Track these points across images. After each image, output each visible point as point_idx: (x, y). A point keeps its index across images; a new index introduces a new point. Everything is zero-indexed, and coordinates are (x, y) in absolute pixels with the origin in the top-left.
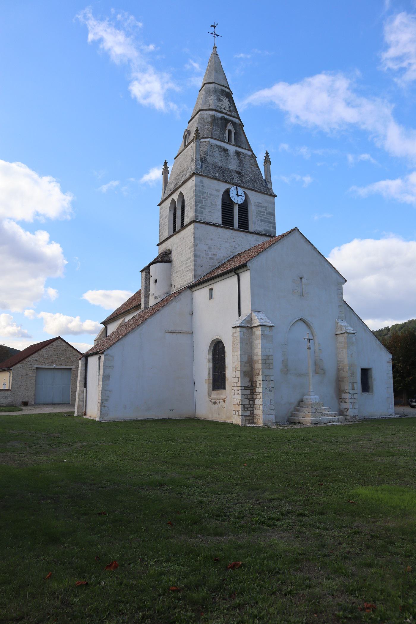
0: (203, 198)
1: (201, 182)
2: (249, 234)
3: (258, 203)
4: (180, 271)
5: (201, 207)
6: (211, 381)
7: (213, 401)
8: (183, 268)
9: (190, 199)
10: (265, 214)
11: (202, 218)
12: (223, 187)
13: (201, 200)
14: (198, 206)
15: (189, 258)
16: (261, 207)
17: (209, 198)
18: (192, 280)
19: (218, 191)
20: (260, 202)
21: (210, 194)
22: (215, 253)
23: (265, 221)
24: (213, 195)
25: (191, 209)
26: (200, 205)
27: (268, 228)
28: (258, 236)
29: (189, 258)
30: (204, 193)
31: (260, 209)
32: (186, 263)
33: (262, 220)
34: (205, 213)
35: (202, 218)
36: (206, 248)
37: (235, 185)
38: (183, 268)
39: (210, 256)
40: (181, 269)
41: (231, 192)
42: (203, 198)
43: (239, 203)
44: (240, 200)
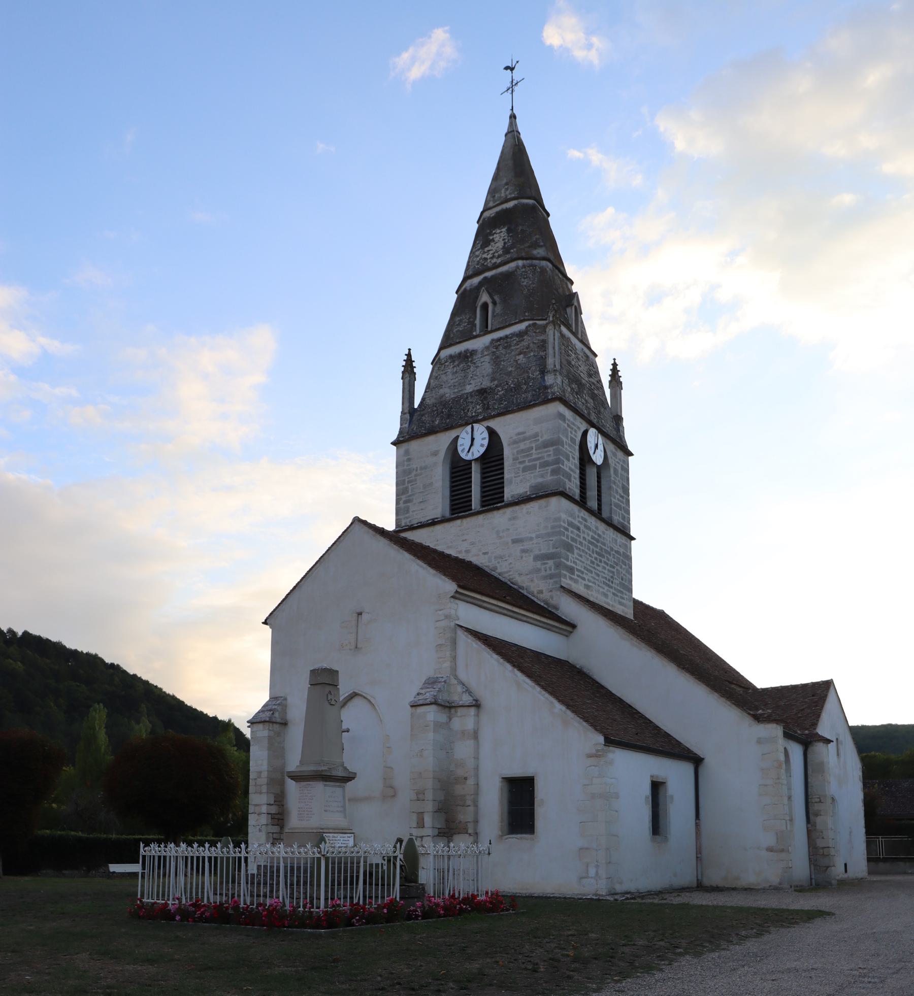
1: (407, 452)
2: (495, 513)
3: (519, 434)
5: (405, 502)
12: (443, 440)
13: (407, 488)
14: (401, 502)
16: (525, 439)
17: (418, 478)
19: (435, 454)
20: (521, 430)
21: (421, 468)
23: (534, 467)
24: (425, 468)
27: (540, 480)
28: (517, 508)
31: (522, 446)
33: (525, 469)
37: (467, 424)
41: (460, 441)
42: (409, 482)
43: (477, 455)
44: (479, 450)
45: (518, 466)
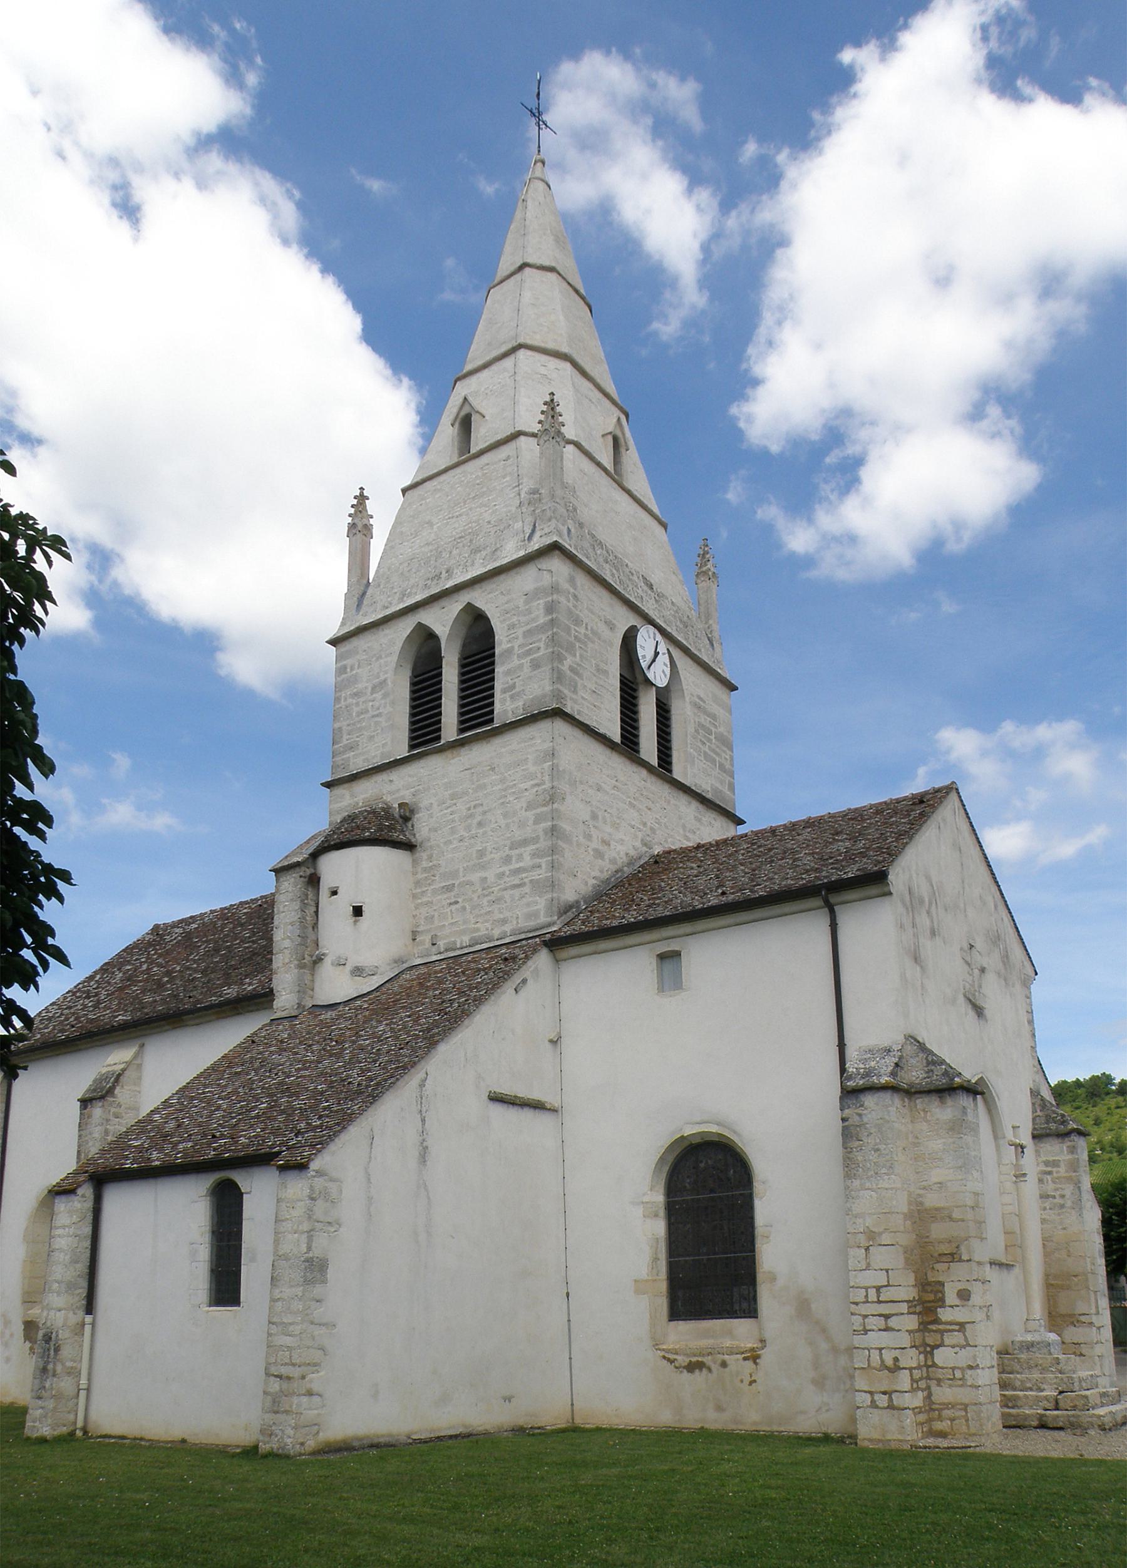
0: (576, 637)
4: (470, 883)
6: (663, 1286)
7: (682, 1360)
8: (491, 875)
9: (529, 633)
10: (713, 737)
11: (576, 707)
15: (525, 842)
17: (590, 645)
18: (543, 919)
22: (606, 837)
25: (536, 665)
26: (569, 661)
27: (718, 785)
29: (525, 842)
30: (578, 622)
32: (507, 860)
34: (581, 693)
35: (576, 707)
36: (584, 813)
38: (491, 875)
39: (595, 844)
40: (475, 877)
45: (699, 744)
